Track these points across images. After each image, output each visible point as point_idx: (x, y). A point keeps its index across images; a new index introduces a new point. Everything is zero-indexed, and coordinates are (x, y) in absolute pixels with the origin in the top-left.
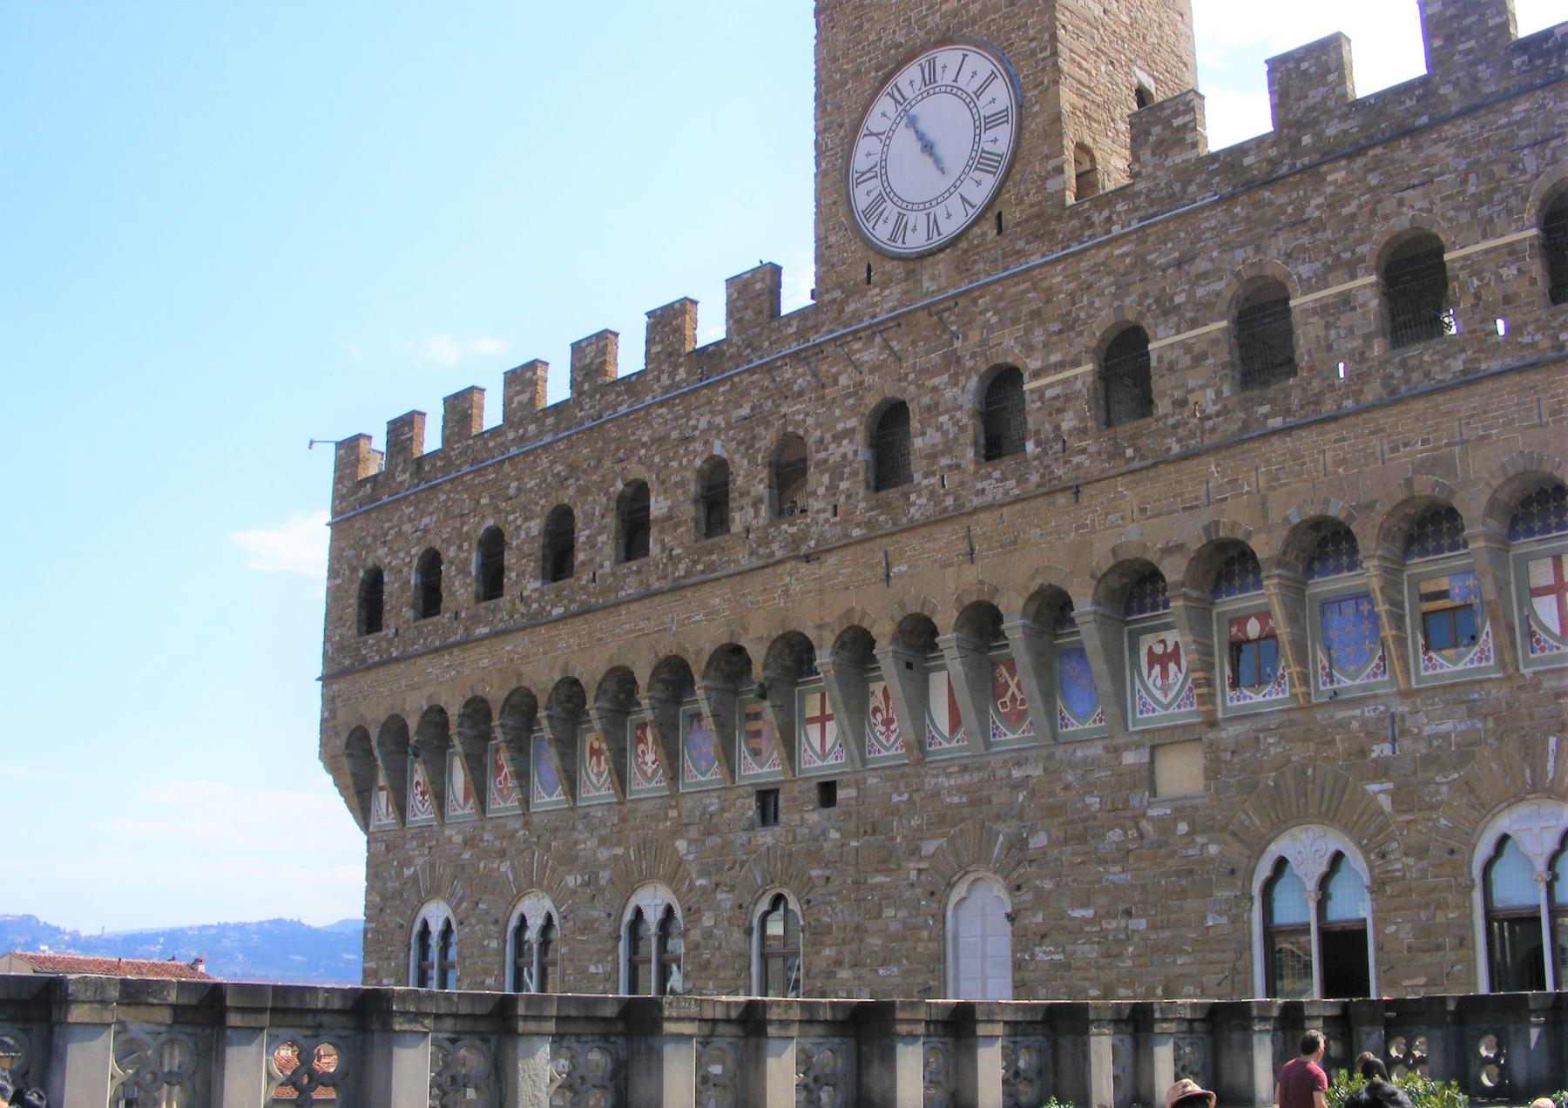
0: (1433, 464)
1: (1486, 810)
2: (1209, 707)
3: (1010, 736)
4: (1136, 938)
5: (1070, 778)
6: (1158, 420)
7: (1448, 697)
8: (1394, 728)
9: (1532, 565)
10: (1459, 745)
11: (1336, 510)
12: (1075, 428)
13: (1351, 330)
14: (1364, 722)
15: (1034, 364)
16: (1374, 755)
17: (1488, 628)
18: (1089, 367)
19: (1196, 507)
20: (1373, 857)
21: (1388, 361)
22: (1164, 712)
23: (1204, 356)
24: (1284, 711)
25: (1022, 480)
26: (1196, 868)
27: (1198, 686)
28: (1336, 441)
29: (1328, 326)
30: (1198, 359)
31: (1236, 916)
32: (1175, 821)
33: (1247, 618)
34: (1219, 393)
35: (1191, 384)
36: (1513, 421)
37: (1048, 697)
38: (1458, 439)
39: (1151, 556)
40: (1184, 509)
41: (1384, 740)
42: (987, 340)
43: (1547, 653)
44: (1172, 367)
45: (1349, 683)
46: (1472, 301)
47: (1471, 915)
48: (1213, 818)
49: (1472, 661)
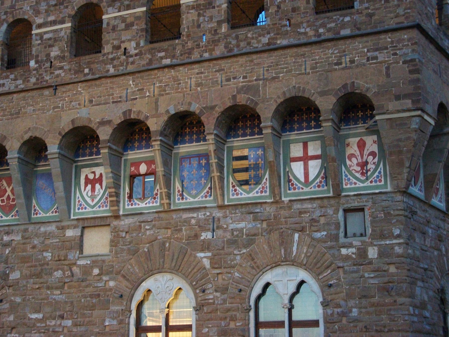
0: (247, 89)
1: (261, 270)
2: (116, 208)
3: (5, 218)
4: (66, 331)
5: (36, 242)
6: (104, 55)
7: (243, 210)
8: (214, 224)
9: (292, 146)
10: (247, 235)
11: (195, 108)
12: (58, 56)
13: (211, 18)
14: (198, 221)
15: (39, 20)
16: (202, 238)
17: (267, 176)
18: (69, 25)
19: (120, 101)
20: (198, 291)
21: (228, 35)
22: (91, 210)
23: (132, 24)
24: (157, 212)
25: (26, 80)
26: (102, 293)
27: (111, 196)
28: (198, 74)
29: (199, 15)
30: (128, 26)
31: (122, 320)
32: (92, 268)
33: (141, 163)
34: (138, 44)
35: (123, 38)
36: (290, 71)
37: (28, 198)
38: (262, 77)
39: (93, 126)
40: (113, 102)
41: (208, 230)
42: (15, 5)
43: (297, 191)
44: (114, 28)
45: (192, 200)
46: (276, 9)
47: (249, 324)
48: (113, 266)
49: (257, 192)
